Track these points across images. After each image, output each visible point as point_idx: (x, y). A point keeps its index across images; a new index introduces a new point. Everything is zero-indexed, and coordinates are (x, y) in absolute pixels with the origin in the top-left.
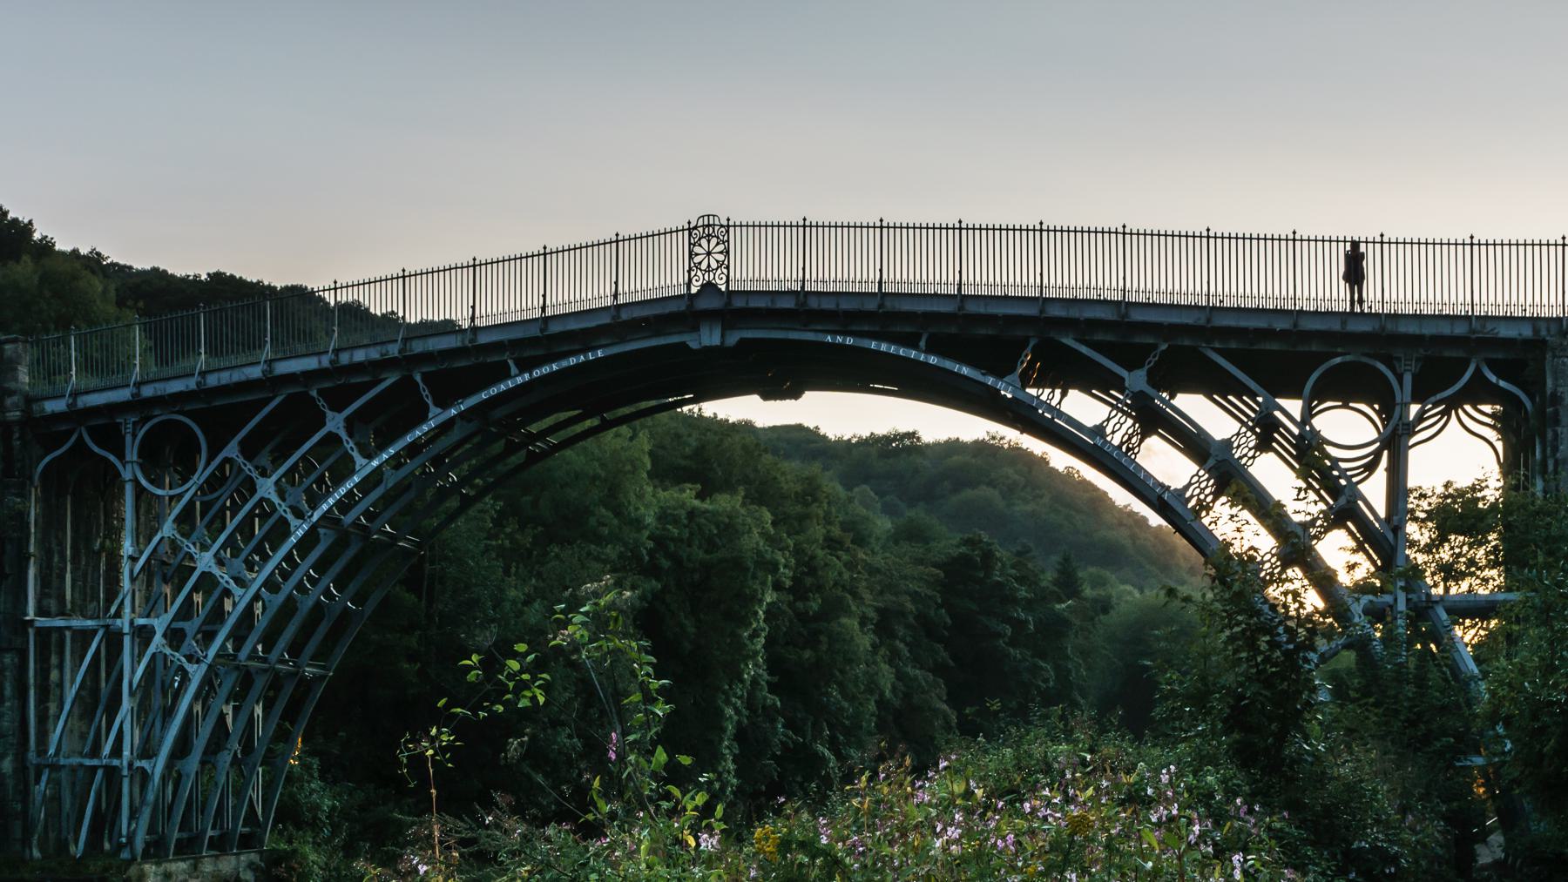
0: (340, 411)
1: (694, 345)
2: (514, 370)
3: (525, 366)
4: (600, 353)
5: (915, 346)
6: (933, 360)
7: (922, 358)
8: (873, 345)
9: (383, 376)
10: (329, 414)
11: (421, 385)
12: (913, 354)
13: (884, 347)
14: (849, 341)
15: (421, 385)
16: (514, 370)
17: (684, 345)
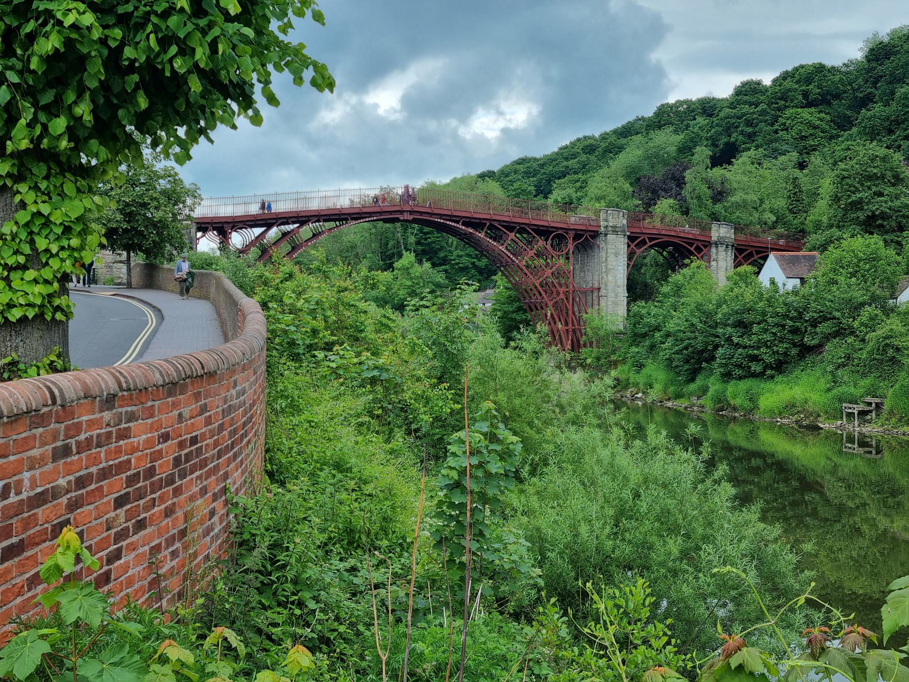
5: (458, 222)
6: (463, 228)
14: (442, 221)
17: (398, 218)
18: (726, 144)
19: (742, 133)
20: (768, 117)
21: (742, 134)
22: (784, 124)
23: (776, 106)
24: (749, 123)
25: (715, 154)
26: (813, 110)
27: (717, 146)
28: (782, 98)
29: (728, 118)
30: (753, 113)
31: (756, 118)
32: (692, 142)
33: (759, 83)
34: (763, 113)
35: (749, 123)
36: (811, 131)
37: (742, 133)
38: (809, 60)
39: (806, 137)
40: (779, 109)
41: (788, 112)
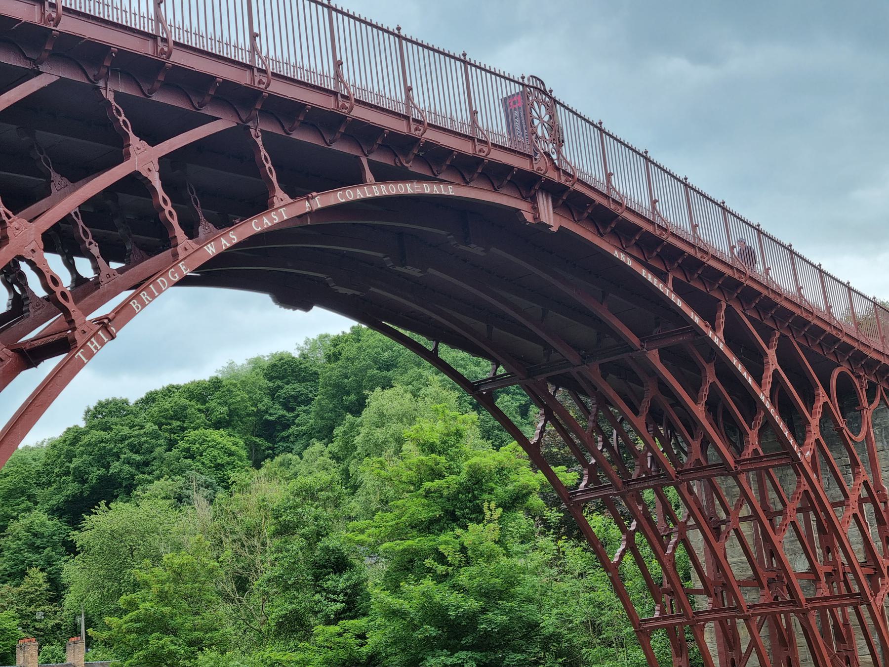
0: (153, 142)
1: (529, 217)
2: (369, 176)
3: (383, 175)
4: (450, 191)
5: (664, 281)
6: (679, 303)
7: (673, 297)
8: (643, 272)
9: (208, 111)
10: (134, 140)
11: (263, 152)
12: (667, 293)
13: (649, 277)
15: (263, 152)
16: (369, 176)
18: (100, 478)
19: (128, 462)
20: (161, 441)
21: (129, 463)
22: (188, 450)
23: (169, 427)
24: (135, 449)
25: (82, 492)
26: (222, 431)
27: (84, 481)
28: (175, 417)
29: (101, 442)
30: (138, 436)
31: (146, 442)
32: (26, 483)
33: (125, 402)
34: (154, 435)
35: (135, 449)
36: (227, 459)
37: (128, 462)
38: (148, 391)
39: (222, 466)
40: (172, 431)
41: (192, 434)
